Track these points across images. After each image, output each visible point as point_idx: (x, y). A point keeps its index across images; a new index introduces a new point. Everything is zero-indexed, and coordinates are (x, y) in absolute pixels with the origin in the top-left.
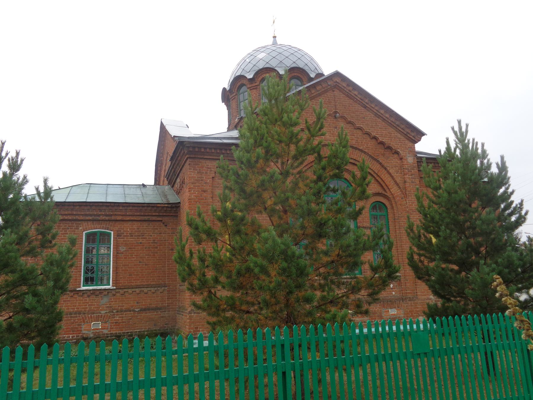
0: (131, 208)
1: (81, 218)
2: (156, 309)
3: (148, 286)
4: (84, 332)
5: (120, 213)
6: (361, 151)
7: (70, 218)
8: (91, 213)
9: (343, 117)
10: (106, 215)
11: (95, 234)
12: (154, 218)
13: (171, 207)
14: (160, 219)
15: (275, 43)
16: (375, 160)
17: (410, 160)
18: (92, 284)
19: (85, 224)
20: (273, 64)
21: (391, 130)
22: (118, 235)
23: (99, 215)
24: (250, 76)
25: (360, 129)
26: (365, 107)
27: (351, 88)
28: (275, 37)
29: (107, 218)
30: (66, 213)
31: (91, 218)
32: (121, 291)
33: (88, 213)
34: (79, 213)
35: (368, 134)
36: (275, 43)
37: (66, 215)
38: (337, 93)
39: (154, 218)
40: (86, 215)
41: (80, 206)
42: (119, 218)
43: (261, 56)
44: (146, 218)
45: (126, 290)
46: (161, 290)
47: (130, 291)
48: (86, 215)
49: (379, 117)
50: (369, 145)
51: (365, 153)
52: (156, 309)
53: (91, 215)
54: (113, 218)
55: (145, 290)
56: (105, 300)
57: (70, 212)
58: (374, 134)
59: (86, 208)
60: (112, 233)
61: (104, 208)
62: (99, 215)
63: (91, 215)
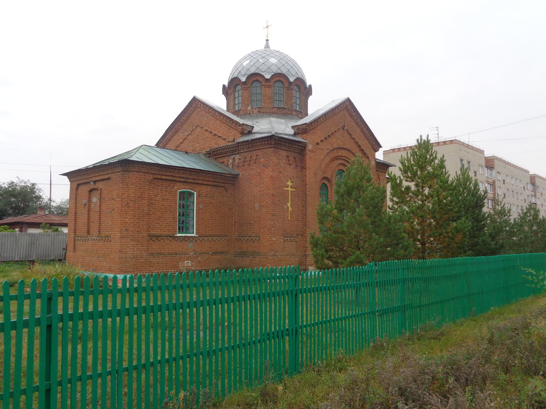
0: (209, 175)
1: (178, 179)
2: (221, 253)
3: (216, 236)
4: (180, 268)
5: (201, 178)
7: (170, 178)
8: (184, 176)
9: (347, 130)
10: (193, 179)
11: (184, 192)
12: (221, 184)
13: (233, 177)
15: (267, 46)
17: (373, 163)
18: (183, 233)
19: (178, 184)
20: (284, 71)
22: (199, 196)
23: (188, 178)
24: (268, 76)
25: (353, 139)
26: (357, 124)
27: (353, 110)
28: (267, 40)
29: (193, 181)
30: (169, 174)
31: (183, 180)
32: (201, 239)
33: (182, 176)
34: (177, 175)
35: (357, 143)
36: (267, 46)
38: (346, 112)
39: (221, 184)
40: (181, 177)
41: (165, 168)
42: (200, 182)
43: (273, 60)
44: (216, 184)
45: (203, 238)
46: (223, 239)
47: (206, 239)
48: (181, 177)
49: (363, 132)
52: (221, 253)
53: (183, 178)
54: (197, 181)
55: (215, 238)
56: (191, 245)
57: (171, 174)
58: (360, 143)
59: (182, 172)
60: (195, 193)
61: (194, 173)
62: (188, 178)
63: (183, 178)
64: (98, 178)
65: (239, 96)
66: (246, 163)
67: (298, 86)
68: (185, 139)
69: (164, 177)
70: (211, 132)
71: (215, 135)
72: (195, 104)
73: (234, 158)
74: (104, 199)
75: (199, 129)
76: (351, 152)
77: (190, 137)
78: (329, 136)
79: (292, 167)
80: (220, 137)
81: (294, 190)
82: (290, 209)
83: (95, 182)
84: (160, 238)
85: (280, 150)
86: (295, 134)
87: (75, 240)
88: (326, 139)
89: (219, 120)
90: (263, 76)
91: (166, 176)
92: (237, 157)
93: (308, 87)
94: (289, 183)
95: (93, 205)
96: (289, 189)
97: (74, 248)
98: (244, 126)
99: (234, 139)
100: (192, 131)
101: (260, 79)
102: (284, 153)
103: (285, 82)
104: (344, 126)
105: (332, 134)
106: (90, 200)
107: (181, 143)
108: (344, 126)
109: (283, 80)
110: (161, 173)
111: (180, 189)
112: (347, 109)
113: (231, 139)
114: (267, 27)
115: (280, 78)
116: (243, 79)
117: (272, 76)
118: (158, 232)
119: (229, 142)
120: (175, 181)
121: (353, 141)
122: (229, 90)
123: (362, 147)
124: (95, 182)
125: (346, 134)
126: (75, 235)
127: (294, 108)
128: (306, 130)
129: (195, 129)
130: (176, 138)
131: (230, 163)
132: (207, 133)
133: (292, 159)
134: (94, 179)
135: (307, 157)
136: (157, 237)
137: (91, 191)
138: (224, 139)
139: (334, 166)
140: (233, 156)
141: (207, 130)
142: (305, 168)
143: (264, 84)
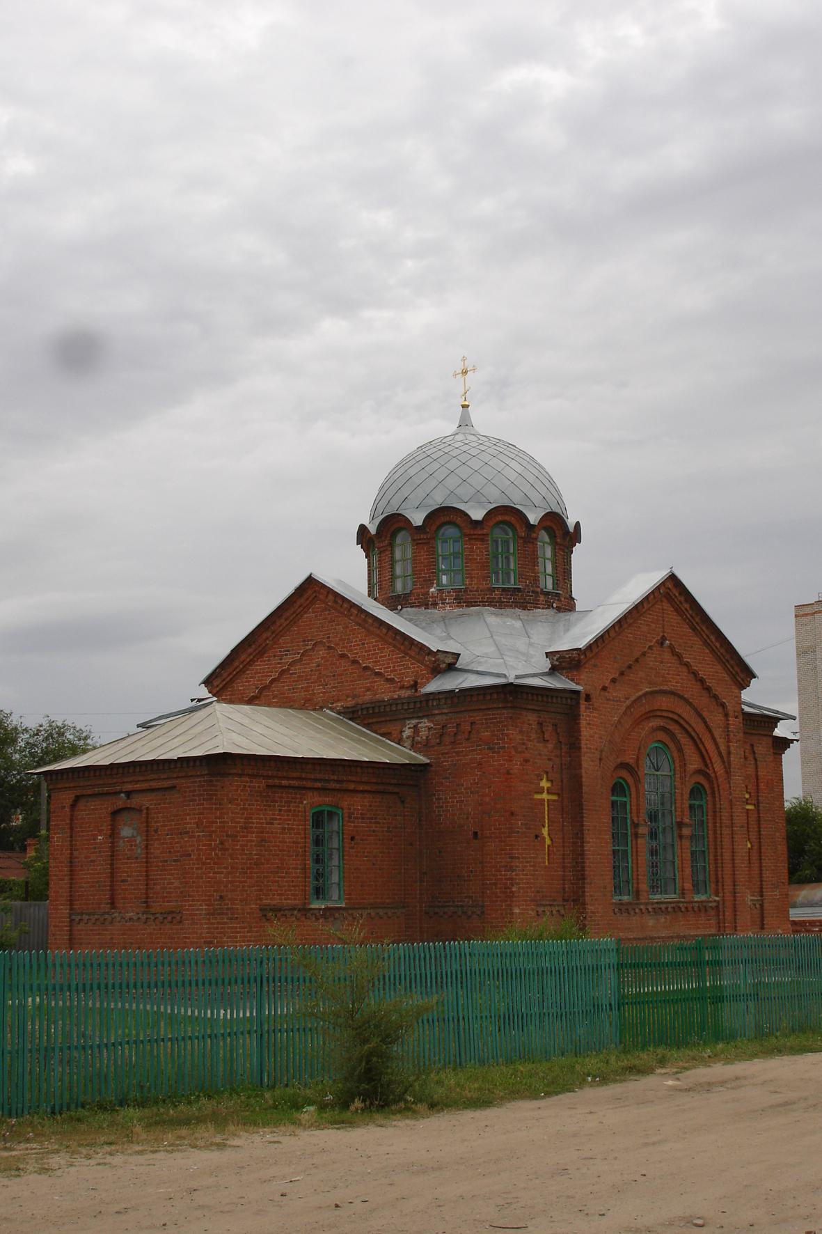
1: (309, 784)
6: (686, 700)
7: (296, 783)
9: (671, 647)
10: (338, 781)
14: (396, 790)
15: (465, 423)
16: (700, 716)
19: (310, 794)
20: (517, 501)
21: (719, 667)
23: (328, 781)
24: (477, 514)
25: (687, 665)
26: (694, 629)
29: (338, 786)
31: (319, 785)
35: (695, 674)
36: (465, 423)
37: (293, 779)
38: (666, 605)
39: (391, 789)
42: (352, 786)
48: (316, 780)
50: (692, 691)
51: (690, 704)
54: (344, 786)
55: (381, 912)
62: (328, 781)
63: (320, 780)
64: (137, 786)
65: (404, 560)
66: (447, 739)
67: (549, 530)
68: (283, 672)
69: (284, 782)
70: (355, 662)
71: (366, 668)
72: (310, 590)
73: (415, 726)
74: (156, 831)
75: (322, 652)
76: (681, 697)
77: (297, 669)
78: (630, 667)
79: (550, 746)
80: (379, 674)
81: (555, 797)
82: (548, 842)
83: (129, 794)
84: (279, 914)
85: (524, 713)
86: (554, 670)
87: (72, 921)
88: (622, 674)
89: (378, 636)
90: (467, 515)
91: (288, 779)
92: (425, 724)
93: (571, 529)
94: (545, 784)
95: (121, 843)
96: (545, 796)
97: (70, 940)
98: (440, 656)
99: (416, 683)
100: (303, 655)
101: (459, 520)
102: (532, 718)
103: (518, 527)
104: (664, 638)
105: (637, 660)
106: (114, 834)
107: (273, 681)
108: (664, 638)
109: (513, 520)
110: (280, 774)
111: (311, 802)
112: (668, 597)
113: (409, 680)
114: (465, 372)
115: (506, 516)
116: (417, 519)
117: (489, 514)
118: (276, 901)
119: (402, 687)
120: (305, 788)
121: (685, 669)
122: (380, 538)
123: (709, 683)
124: (129, 794)
125: (667, 655)
126: (71, 909)
127: (542, 585)
128: (579, 661)
129: (313, 649)
130: (259, 666)
131: (405, 735)
132: (344, 664)
133: (550, 728)
134: (129, 787)
135: (583, 723)
136: (277, 910)
137: (115, 813)
138: (391, 681)
139: (643, 733)
140: (414, 721)
141: (343, 656)
142: (580, 748)
143: (467, 531)
